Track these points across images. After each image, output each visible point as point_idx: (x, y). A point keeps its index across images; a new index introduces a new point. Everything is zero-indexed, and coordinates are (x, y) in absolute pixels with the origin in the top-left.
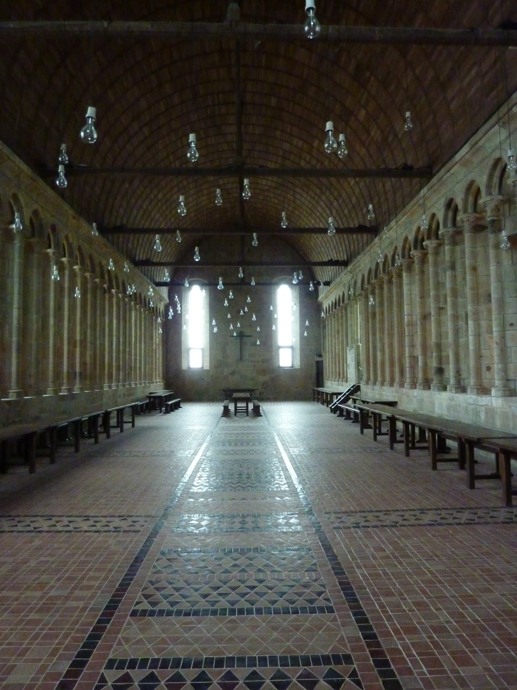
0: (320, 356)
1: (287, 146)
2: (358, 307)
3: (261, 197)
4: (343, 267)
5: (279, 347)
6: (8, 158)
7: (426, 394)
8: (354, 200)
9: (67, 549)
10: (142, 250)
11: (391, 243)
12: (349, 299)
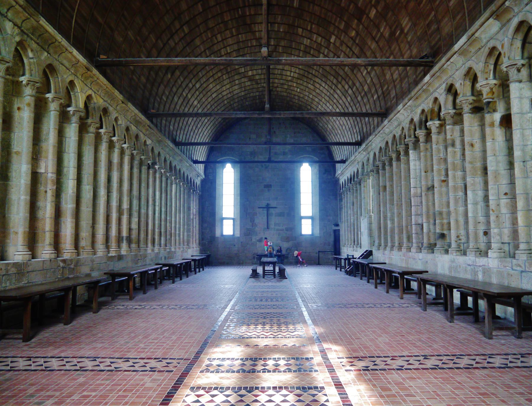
0: (337, 225)
1: (307, 42)
2: (370, 181)
3: (286, 87)
4: (357, 147)
6: (66, 50)
7: (430, 256)
8: (366, 88)
9: (108, 385)
10: (182, 132)
11: (399, 125)
12: (362, 175)
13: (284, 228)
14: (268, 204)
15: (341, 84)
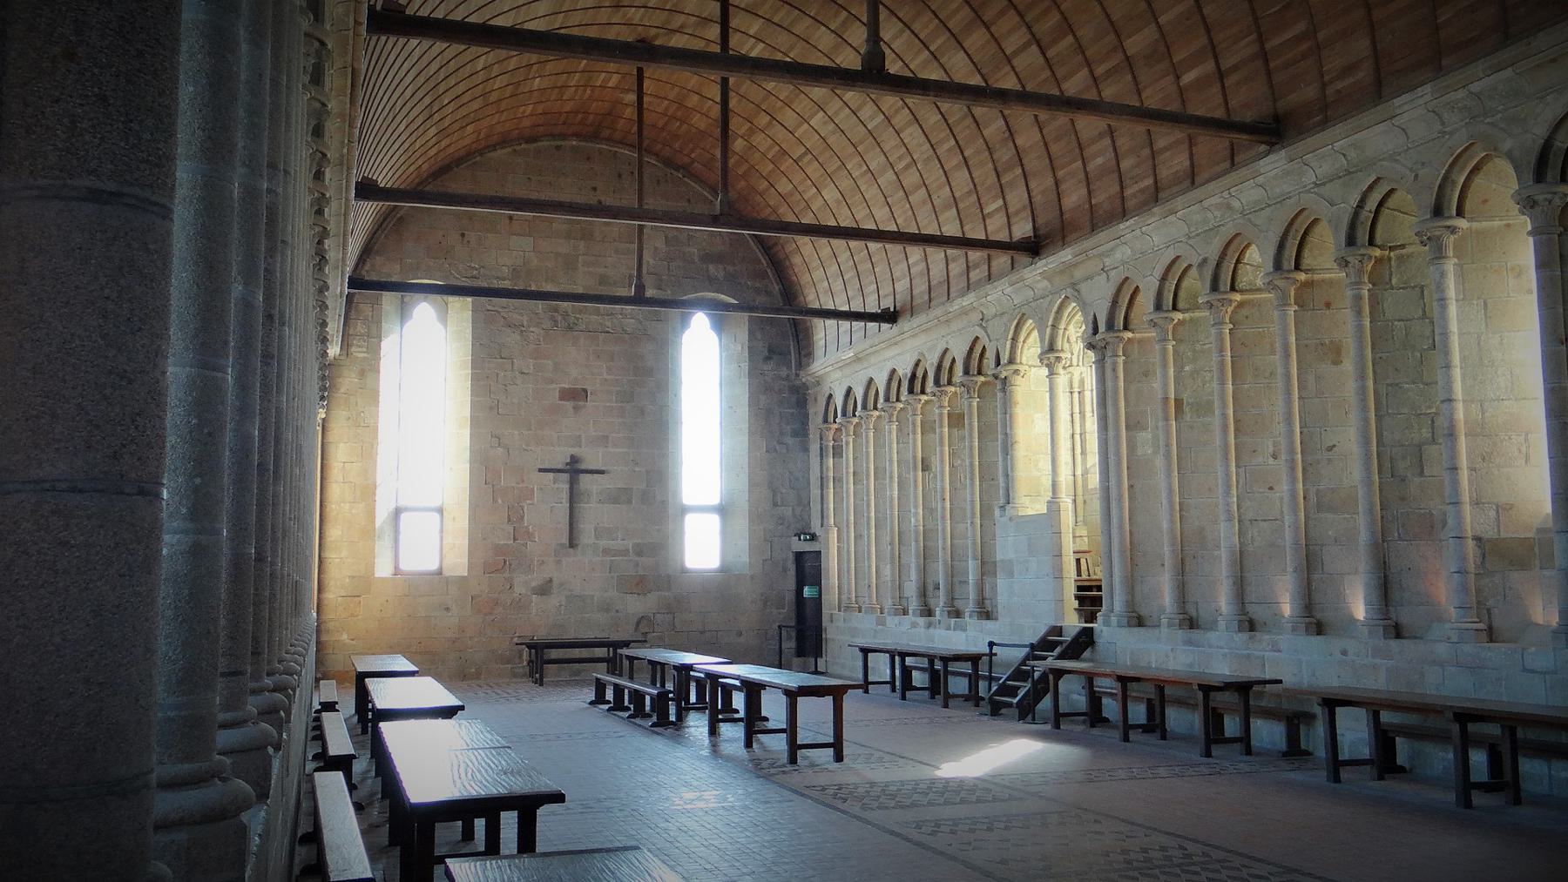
5: (684, 510)
13: (629, 544)
14: (574, 460)
15: (988, 28)
